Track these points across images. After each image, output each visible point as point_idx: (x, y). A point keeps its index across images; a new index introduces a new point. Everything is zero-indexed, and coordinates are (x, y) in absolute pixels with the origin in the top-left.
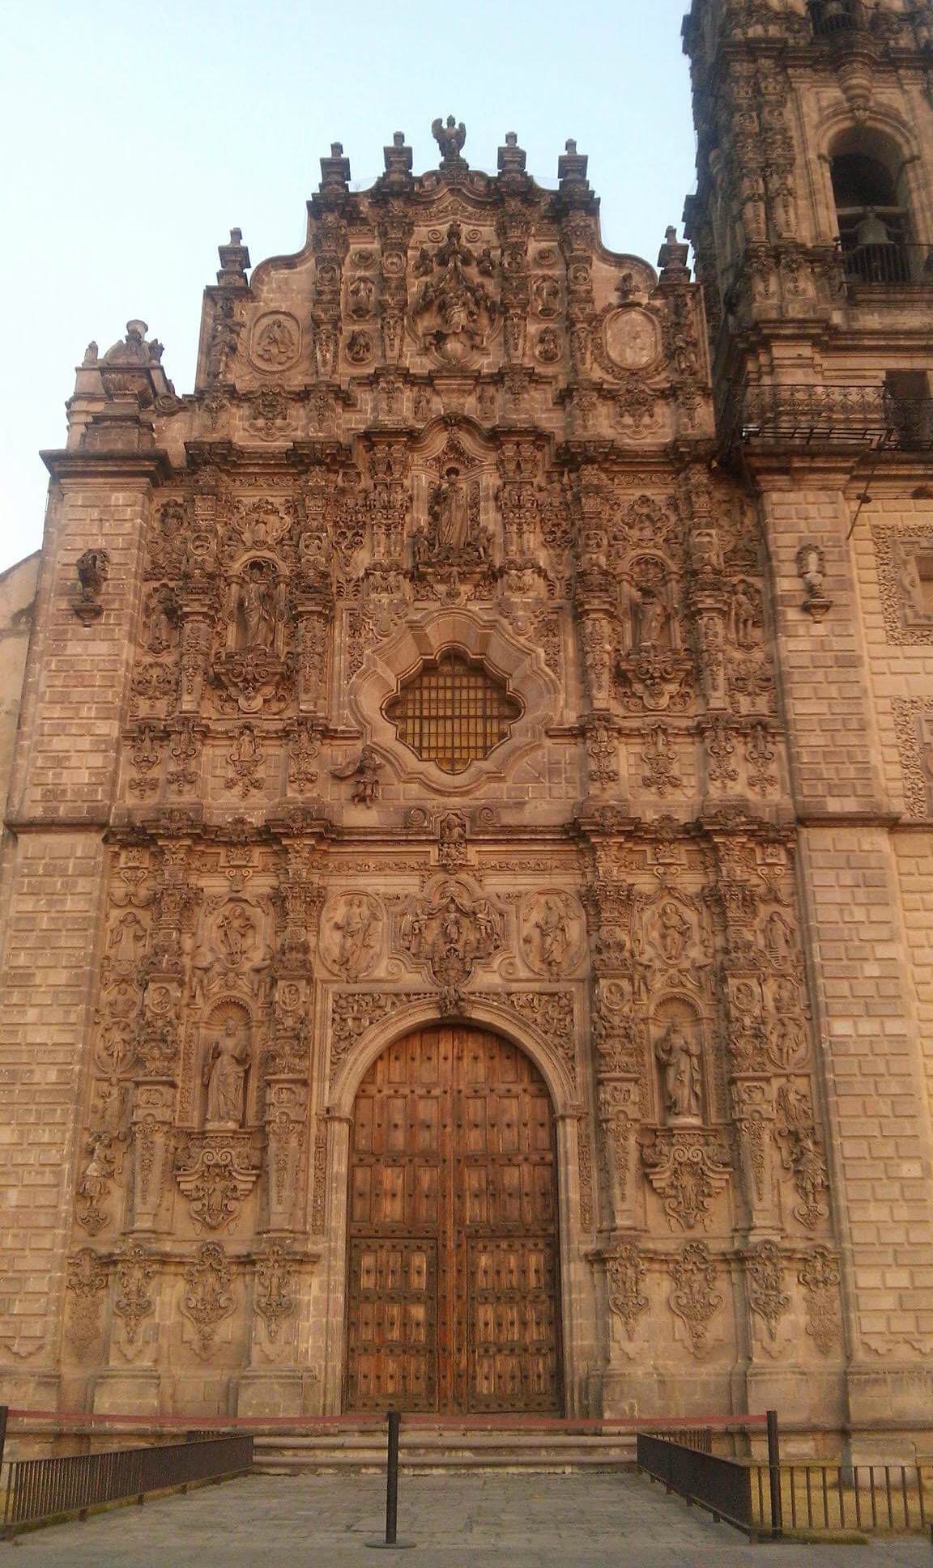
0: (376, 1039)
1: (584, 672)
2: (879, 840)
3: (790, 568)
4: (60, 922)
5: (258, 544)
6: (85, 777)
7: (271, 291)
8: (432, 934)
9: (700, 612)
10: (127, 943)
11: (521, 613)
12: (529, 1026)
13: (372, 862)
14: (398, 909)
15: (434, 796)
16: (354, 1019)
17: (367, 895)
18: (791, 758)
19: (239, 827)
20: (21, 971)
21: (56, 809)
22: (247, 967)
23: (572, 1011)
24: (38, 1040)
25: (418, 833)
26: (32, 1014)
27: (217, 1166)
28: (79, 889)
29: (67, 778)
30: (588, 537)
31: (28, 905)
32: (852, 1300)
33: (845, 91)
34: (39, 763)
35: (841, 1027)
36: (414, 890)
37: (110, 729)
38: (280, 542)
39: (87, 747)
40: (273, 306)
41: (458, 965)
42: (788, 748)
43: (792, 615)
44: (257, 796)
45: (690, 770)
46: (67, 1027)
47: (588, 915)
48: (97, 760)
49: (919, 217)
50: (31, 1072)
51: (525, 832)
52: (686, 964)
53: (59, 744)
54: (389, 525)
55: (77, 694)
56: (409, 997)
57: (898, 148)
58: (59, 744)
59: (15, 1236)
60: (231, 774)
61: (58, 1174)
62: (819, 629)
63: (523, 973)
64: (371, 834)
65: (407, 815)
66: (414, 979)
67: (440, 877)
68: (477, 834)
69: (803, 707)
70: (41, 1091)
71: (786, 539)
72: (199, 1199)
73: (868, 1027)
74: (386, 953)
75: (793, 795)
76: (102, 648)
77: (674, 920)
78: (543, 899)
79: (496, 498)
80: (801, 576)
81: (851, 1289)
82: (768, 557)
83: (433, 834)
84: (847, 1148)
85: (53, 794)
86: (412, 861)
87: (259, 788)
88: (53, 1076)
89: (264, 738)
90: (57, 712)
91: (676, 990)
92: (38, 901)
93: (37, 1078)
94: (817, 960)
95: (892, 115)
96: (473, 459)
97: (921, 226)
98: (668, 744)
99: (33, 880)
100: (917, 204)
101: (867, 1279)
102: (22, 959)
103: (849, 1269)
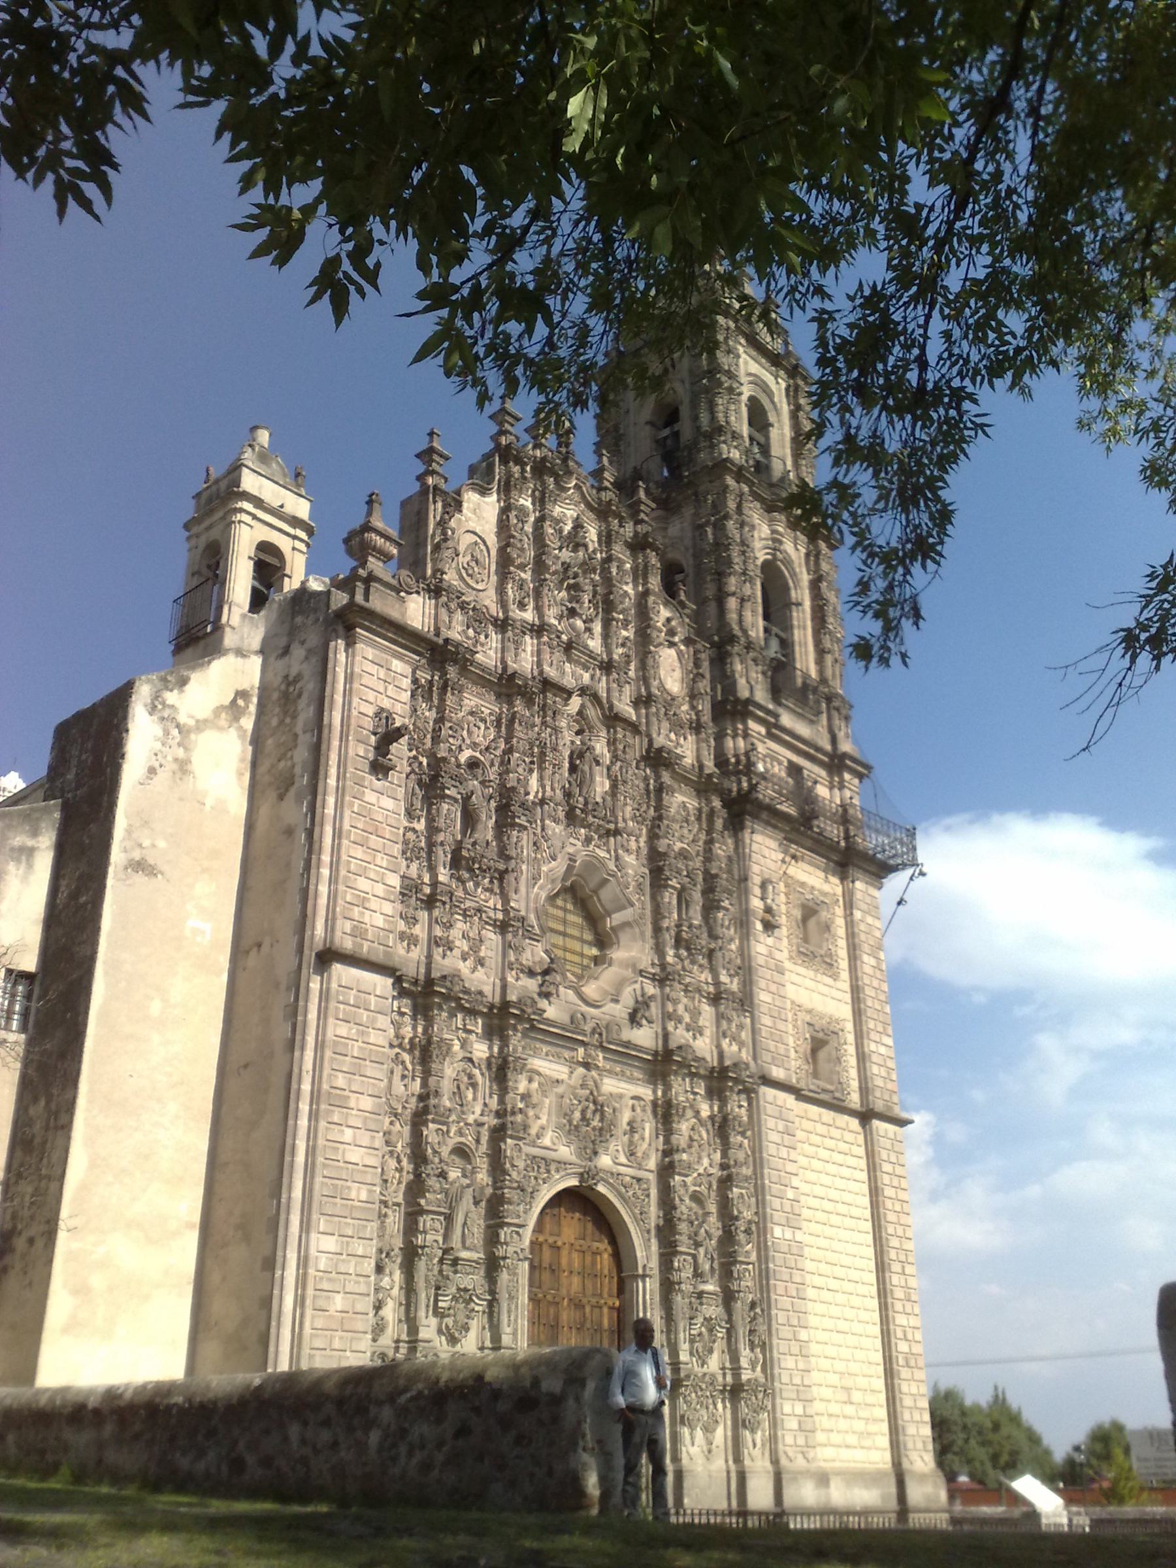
0: (546, 1194)
1: (657, 930)
2: (789, 1100)
3: (757, 891)
4: (367, 1052)
5: (474, 746)
6: (380, 921)
7: (468, 508)
8: (577, 1115)
9: (719, 908)
10: (397, 1078)
11: (630, 871)
12: (627, 1203)
13: (545, 1048)
14: (560, 1089)
15: (580, 1003)
16: (536, 1178)
17: (539, 1074)
18: (754, 1031)
19: (479, 997)
20: (338, 1092)
21: (362, 945)
22: (471, 1119)
23: (648, 1196)
24: (353, 1161)
25: (579, 1034)
26: (348, 1134)
27: (466, 1290)
28: (379, 1026)
29: (367, 919)
30: (668, 826)
31: (343, 1030)
32: (779, 1422)
33: (774, 532)
34: (348, 898)
35: (778, 1231)
36: (564, 1077)
37: (395, 881)
38: (487, 749)
39: (381, 894)
40: (472, 525)
41: (591, 1145)
42: (753, 1023)
43: (759, 926)
44: (480, 973)
45: (707, 1024)
46: (371, 1151)
47: (657, 1123)
48: (388, 908)
49: (797, 648)
50: (349, 1188)
51: (634, 1050)
52: (701, 1171)
53: (363, 884)
54: (555, 765)
55: (374, 841)
56: (562, 1164)
57: (787, 589)
58: (363, 884)
59: (341, 1338)
60: (466, 949)
61: (368, 1284)
62: (770, 941)
63: (623, 1159)
64: (555, 1027)
65: (572, 1019)
66: (565, 1152)
67: (581, 1070)
68: (610, 1043)
69: (762, 997)
70: (356, 1207)
71: (755, 868)
72: (448, 1316)
73: (788, 1235)
74: (552, 1127)
75: (755, 1058)
76: (388, 803)
77: (696, 1137)
78: (631, 1102)
79: (609, 769)
80: (762, 899)
81: (778, 1415)
82: (745, 879)
83: (585, 1035)
84: (780, 1317)
85: (358, 932)
86: (567, 1054)
87: (482, 965)
88: (364, 1196)
89: (487, 923)
90: (359, 852)
91: (697, 1189)
92: (351, 1029)
93: (353, 1195)
94: (767, 1182)
95: (788, 562)
96: (593, 727)
97: (797, 656)
98: (700, 1001)
99: (348, 1008)
100: (796, 638)
101: (787, 1408)
102: (340, 1081)
103: (778, 1401)
